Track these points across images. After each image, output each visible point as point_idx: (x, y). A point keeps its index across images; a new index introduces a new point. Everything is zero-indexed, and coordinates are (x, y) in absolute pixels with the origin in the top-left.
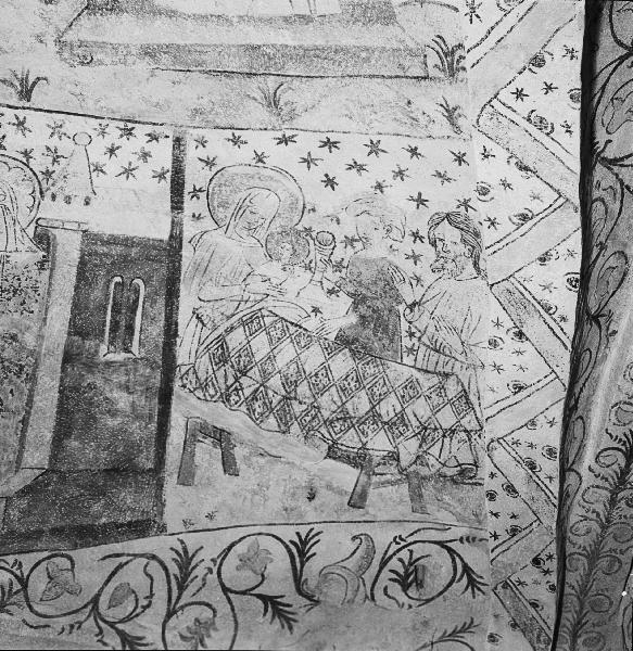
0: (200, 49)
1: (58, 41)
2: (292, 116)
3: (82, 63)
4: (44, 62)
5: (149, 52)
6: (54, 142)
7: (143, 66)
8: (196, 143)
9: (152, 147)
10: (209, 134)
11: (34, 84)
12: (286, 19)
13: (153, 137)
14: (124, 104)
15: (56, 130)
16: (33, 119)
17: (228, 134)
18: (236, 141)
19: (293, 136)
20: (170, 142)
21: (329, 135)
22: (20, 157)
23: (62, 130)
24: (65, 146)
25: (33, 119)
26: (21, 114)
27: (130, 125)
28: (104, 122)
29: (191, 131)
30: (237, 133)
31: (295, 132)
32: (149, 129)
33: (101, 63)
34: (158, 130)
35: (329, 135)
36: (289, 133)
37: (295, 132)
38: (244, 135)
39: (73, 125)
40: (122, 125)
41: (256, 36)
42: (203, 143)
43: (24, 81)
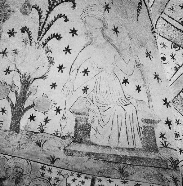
0: (103, 155)
1: (65, 150)
2: (127, 176)
3: (70, 155)
4: (60, 154)
5: (88, 154)
6: (57, 176)
7: (86, 158)
8: (98, 181)
9: (86, 181)
10: (102, 178)
11: (56, 159)
12: (127, 149)
13: (86, 178)
14: (78, 167)
15: (59, 173)
16: (55, 170)
17: (108, 179)
18: (110, 181)
19: (127, 182)
20: (91, 179)
21: (138, 182)
22: (48, 179)
23: (61, 173)
24: (61, 177)
25: (55, 170)
26: (51, 168)
27: (80, 174)
28: (73, 172)
29: (97, 177)
30: (111, 179)
31: (128, 181)
32: (85, 175)
33: (75, 156)
34: (88, 176)
35: (138, 182)
36: (126, 181)
37: (128, 181)
38: (113, 180)
39: (64, 172)
40: (78, 173)
41: (118, 153)
42: (100, 181)
43: (53, 158)
